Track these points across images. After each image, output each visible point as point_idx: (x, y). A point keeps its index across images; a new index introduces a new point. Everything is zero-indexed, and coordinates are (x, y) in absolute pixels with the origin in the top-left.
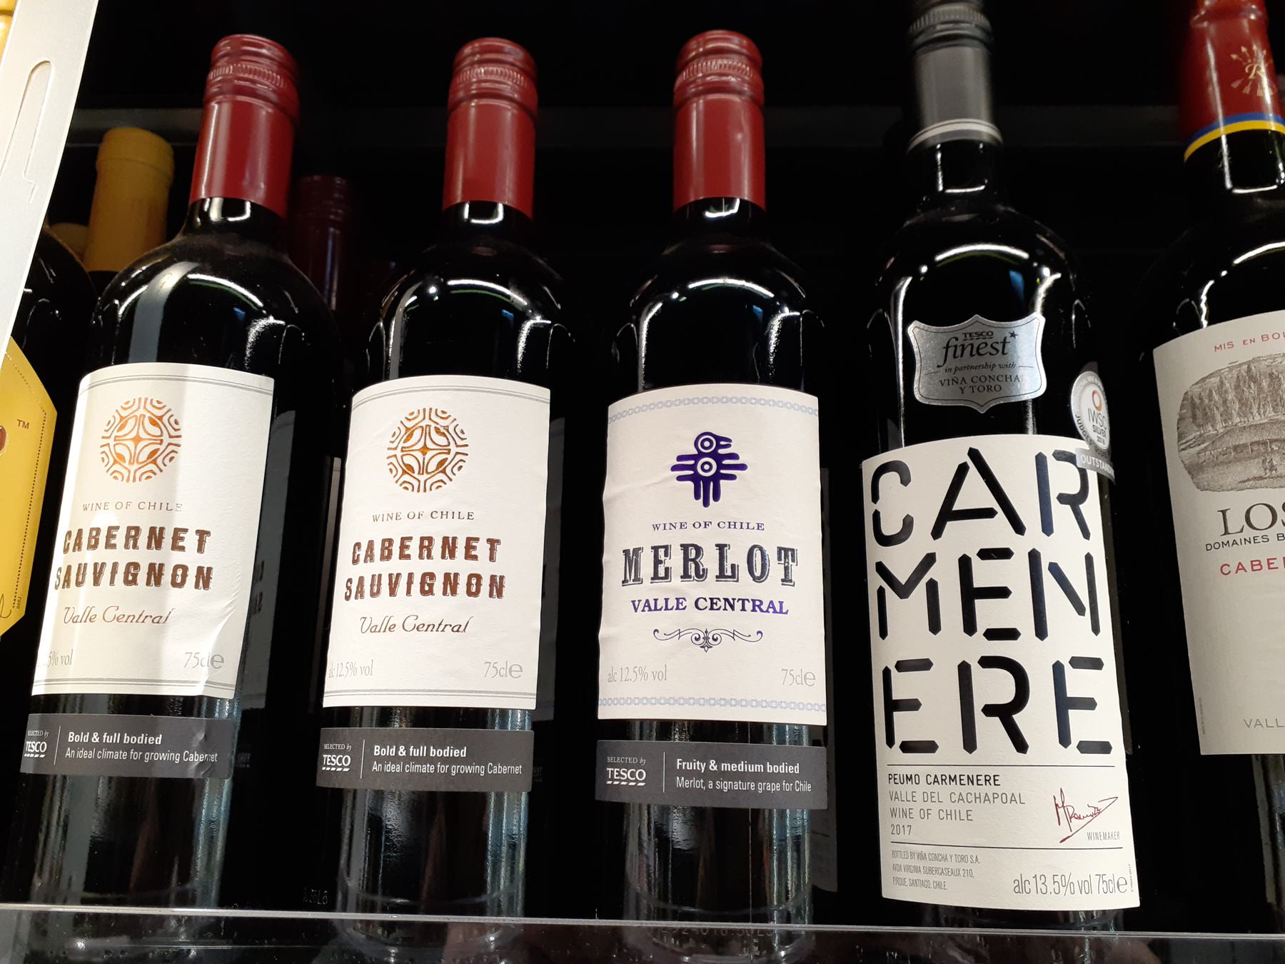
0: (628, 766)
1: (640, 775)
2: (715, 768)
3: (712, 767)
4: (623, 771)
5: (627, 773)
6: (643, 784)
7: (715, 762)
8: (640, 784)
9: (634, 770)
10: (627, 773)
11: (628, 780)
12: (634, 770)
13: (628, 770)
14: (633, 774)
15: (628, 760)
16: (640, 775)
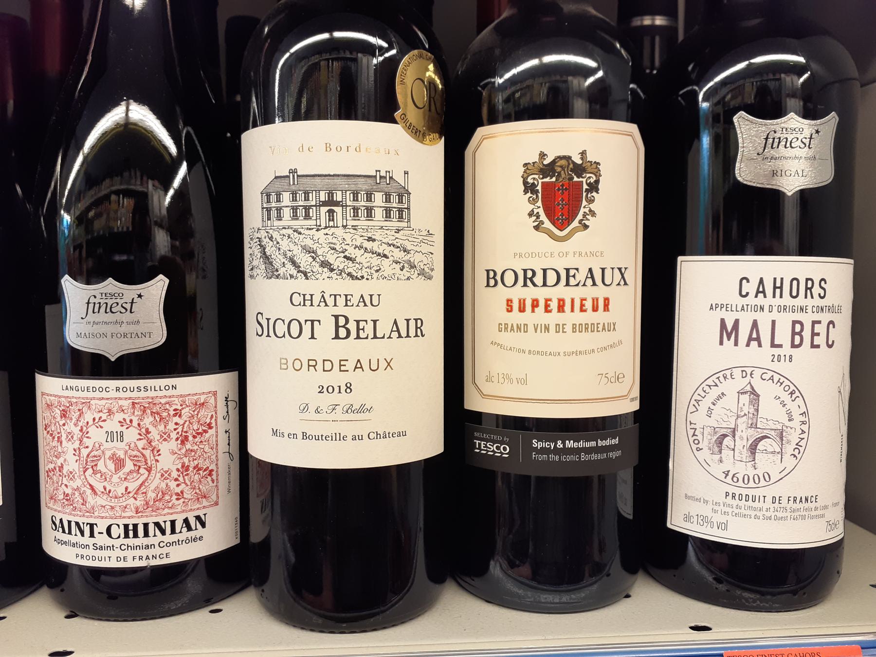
0: (494, 442)
1: (505, 449)
2: (561, 446)
3: (559, 446)
4: (489, 445)
5: (493, 446)
6: (507, 456)
7: (561, 442)
8: (504, 456)
9: (499, 445)
10: (493, 446)
11: (493, 451)
12: (499, 445)
13: (494, 444)
14: (498, 448)
15: (493, 437)
16: (505, 449)
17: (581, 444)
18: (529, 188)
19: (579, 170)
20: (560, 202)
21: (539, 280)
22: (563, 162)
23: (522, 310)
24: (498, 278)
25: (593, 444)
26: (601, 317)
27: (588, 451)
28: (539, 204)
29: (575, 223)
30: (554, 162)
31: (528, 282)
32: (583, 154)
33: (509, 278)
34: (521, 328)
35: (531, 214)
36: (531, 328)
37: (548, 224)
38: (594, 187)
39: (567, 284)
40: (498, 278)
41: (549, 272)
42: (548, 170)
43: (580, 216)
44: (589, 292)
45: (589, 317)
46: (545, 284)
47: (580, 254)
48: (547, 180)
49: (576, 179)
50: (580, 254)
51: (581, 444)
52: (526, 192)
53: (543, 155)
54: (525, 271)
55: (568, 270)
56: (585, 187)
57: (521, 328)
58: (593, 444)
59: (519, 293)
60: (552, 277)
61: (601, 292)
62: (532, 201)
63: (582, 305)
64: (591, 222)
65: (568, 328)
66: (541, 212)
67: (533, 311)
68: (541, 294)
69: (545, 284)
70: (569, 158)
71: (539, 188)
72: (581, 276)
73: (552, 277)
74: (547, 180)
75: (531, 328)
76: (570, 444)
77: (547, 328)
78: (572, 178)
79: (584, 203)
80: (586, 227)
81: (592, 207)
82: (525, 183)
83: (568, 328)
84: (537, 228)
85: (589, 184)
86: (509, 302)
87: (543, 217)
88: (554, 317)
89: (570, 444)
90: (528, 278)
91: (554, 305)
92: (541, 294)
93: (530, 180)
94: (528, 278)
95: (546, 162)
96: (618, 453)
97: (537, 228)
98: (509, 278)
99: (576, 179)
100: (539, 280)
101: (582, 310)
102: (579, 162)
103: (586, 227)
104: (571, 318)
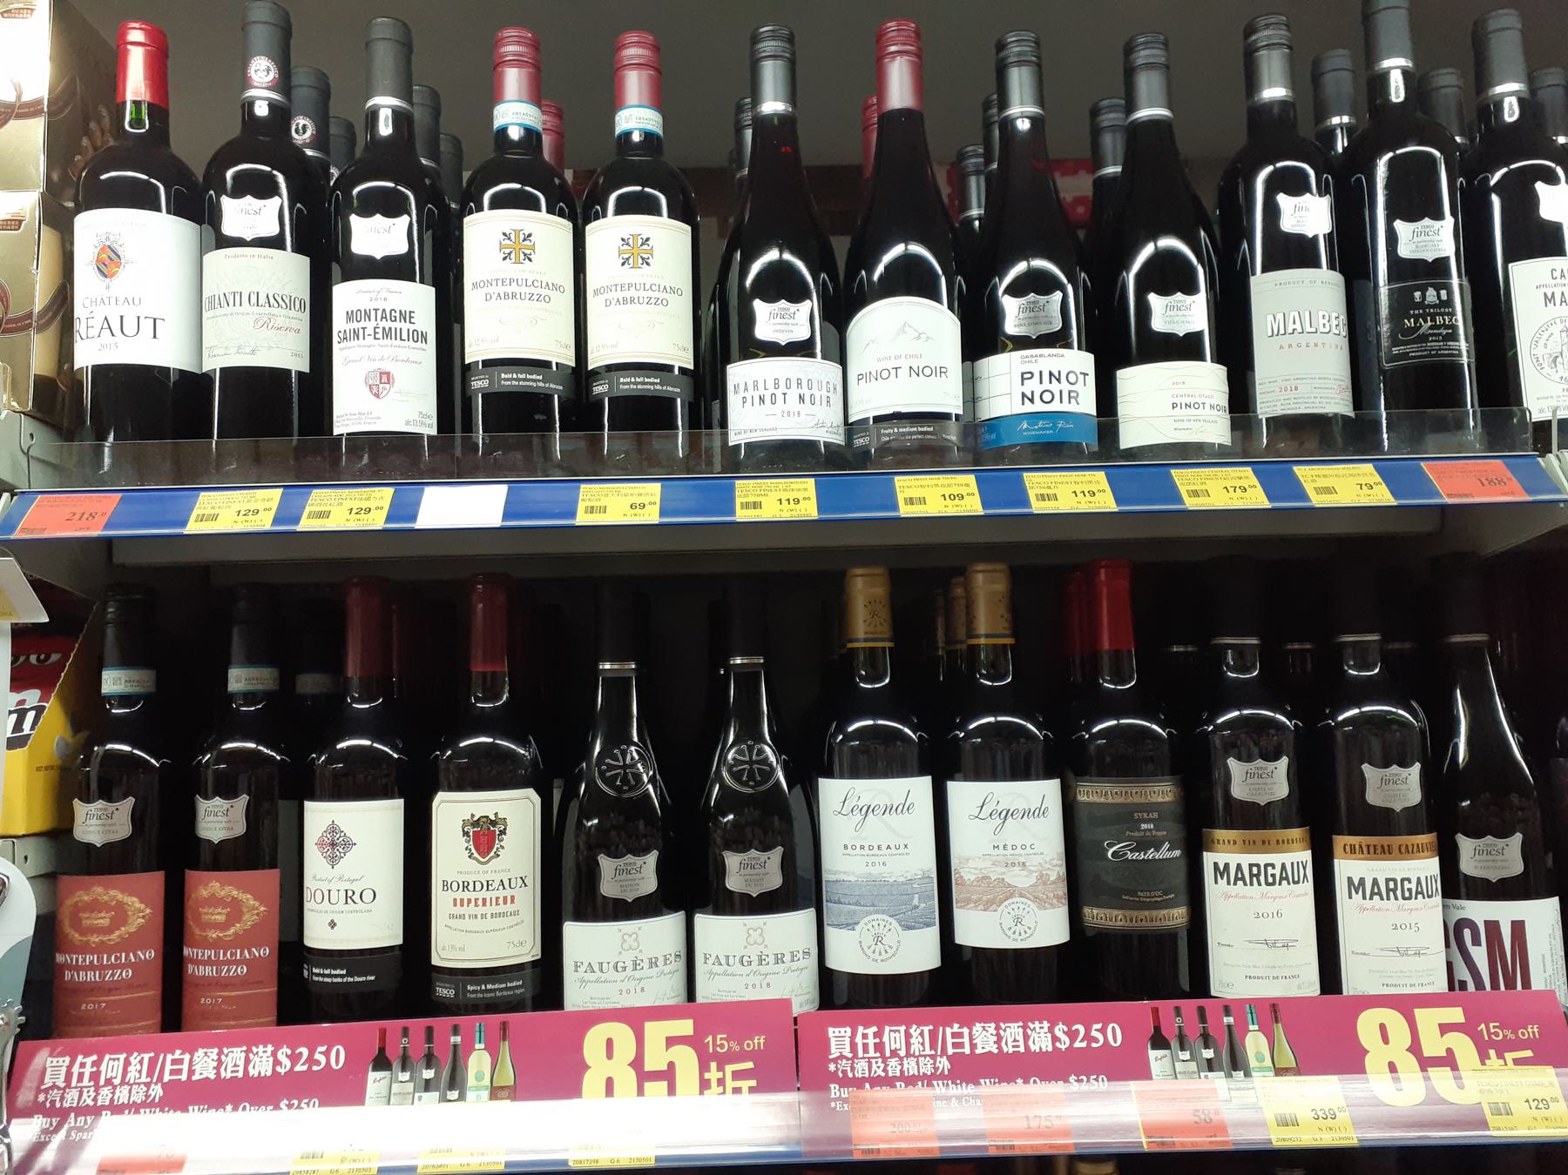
17: (496, 986)
18: (466, 834)
19: (494, 823)
20: (483, 840)
21: (471, 888)
22: (484, 820)
23: (462, 905)
24: (449, 885)
25: (504, 985)
26: (509, 907)
27: (501, 990)
28: (471, 843)
29: (492, 854)
30: (479, 819)
31: (465, 889)
32: (496, 814)
33: (455, 886)
34: (462, 917)
35: (466, 849)
36: (467, 917)
37: (476, 855)
38: (503, 832)
39: (488, 889)
40: (449, 885)
41: (477, 883)
42: (476, 824)
43: (495, 850)
44: (501, 893)
45: (502, 908)
46: (474, 890)
47: (495, 872)
48: (475, 829)
49: (492, 829)
50: (495, 872)
51: (496, 986)
52: (464, 836)
53: (473, 816)
54: (464, 882)
55: (488, 882)
56: (498, 833)
57: (462, 917)
58: (504, 985)
59: (460, 895)
60: (478, 886)
61: (508, 893)
62: (469, 842)
63: (497, 901)
64: (501, 852)
65: (489, 916)
66: (472, 847)
67: (468, 906)
68: (473, 896)
69: (474, 890)
70: (488, 817)
71: (471, 834)
72: (496, 884)
73: (478, 886)
74: (475, 829)
75: (467, 917)
76: (489, 987)
77: (476, 916)
78: (489, 829)
79: (497, 842)
80: (498, 856)
81: (502, 843)
82: (463, 831)
83: (489, 916)
84: (470, 857)
85: (500, 831)
86: (455, 900)
87: (473, 851)
88: (480, 910)
89: (489, 987)
90: (465, 887)
91: (480, 902)
92: (473, 896)
93: (466, 829)
94: (465, 887)
95: (475, 819)
96: (522, 990)
97: (470, 857)
98: (455, 886)
99: (492, 829)
100: (471, 888)
101: (497, 904)
102: (493, 818)
103: (498, 856)
104: (488, 910)
